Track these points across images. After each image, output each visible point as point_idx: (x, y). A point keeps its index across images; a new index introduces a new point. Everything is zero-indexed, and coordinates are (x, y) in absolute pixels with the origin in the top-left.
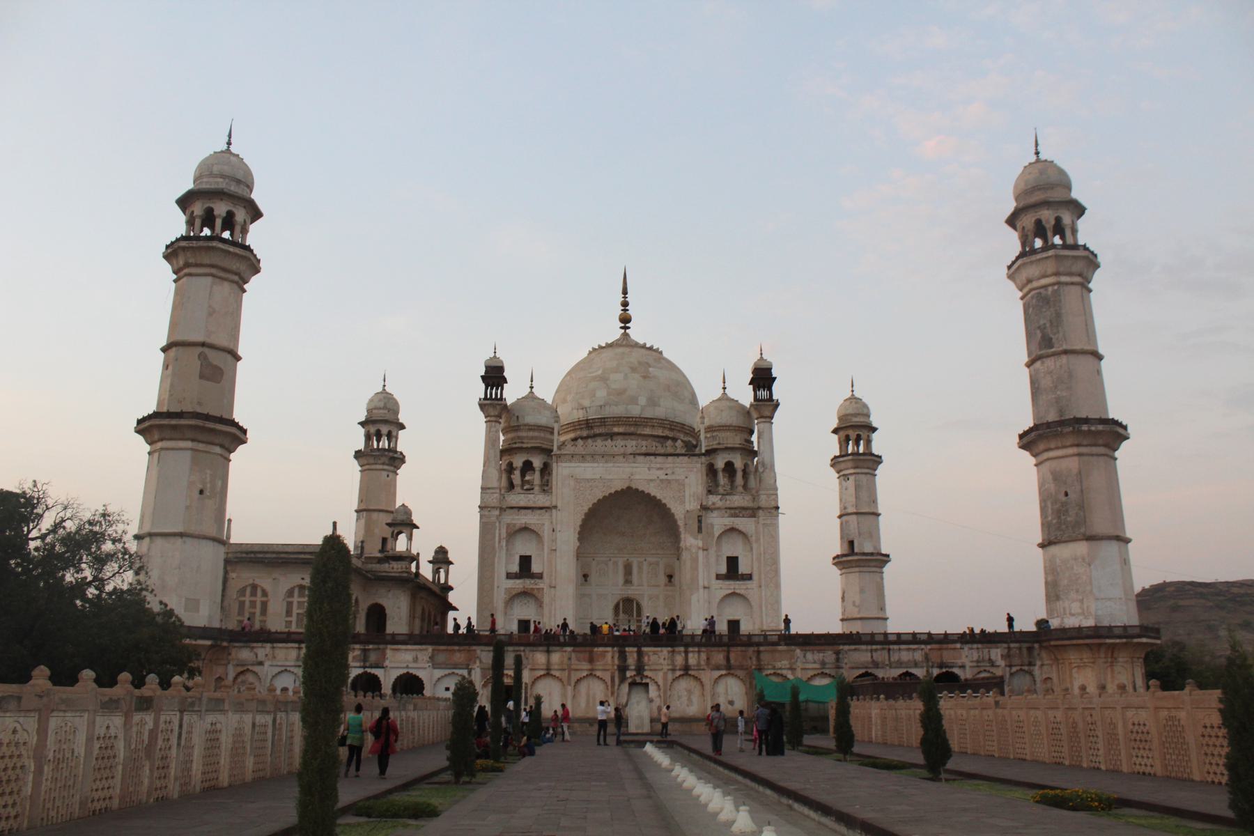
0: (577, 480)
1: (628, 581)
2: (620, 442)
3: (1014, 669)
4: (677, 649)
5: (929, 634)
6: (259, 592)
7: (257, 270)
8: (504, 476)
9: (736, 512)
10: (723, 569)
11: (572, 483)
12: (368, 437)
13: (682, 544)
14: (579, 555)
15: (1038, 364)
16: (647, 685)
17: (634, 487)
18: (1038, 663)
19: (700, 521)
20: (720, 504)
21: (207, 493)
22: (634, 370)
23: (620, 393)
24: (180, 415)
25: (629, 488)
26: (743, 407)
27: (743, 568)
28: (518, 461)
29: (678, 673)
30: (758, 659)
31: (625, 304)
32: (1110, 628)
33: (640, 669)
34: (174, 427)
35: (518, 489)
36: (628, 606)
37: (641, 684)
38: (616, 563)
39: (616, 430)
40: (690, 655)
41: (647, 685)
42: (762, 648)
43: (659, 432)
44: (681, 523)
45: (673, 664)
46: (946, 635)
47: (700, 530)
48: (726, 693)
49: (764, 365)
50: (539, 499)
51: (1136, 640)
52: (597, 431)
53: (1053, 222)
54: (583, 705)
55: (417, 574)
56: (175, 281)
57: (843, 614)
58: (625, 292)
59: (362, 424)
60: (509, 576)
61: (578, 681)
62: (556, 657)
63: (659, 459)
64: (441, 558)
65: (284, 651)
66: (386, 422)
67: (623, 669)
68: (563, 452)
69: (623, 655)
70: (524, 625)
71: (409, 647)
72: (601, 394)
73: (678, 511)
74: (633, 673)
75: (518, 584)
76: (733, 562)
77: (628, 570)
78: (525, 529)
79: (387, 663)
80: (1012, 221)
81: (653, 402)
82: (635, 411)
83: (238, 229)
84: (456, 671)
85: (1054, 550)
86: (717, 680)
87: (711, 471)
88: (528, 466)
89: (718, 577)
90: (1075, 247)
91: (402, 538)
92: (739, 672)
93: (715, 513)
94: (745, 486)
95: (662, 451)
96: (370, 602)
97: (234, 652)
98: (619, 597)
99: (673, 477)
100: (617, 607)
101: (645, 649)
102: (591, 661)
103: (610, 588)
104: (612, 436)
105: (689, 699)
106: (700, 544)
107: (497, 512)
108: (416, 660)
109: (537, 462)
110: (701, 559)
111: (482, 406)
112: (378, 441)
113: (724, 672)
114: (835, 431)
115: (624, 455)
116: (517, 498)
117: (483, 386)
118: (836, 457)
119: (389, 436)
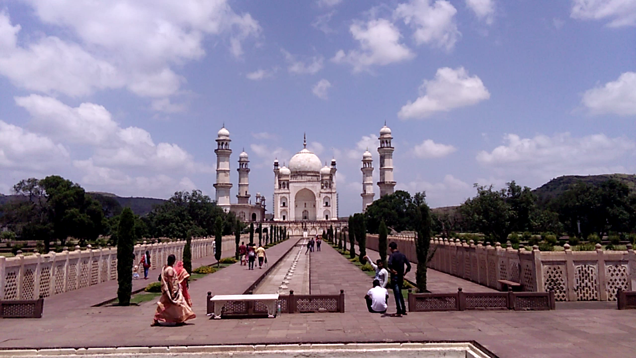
1: (305, 207)
2: (303, 177)
7: (231, 153)
14: (295, 201)
19: (320, 195)
23: (304, 165)
24: (223, 184)
25: (305, 189)
27: (328, 205)
28: (282, 183)
31: (305, 141)
33: (305, 227)
35: (282, 188)
43: (312, 174)
47: (320, 197)
49: (334, 160)
50: (288, 191)
58: (305, 138)
60: (281, 207)
62: (291, 225)
64: (263, 200)
67: (302, 227)
69: (302, 224)
72: (299, 165)
73: (315, 193)
75: (283, 208)
76: (327, 203)
77: (305, 204)
78: (284, 197)
81: (311, 167)
82: (307, 170)
88: (284, 184)
89: (324, 206)
91: (258, 199)
95: (311, 180)
100: (303, 212)
102: (297, 225)
103: (301, 209)
104: (302, 176)
109: (286, 183)
115: (304, 182)
116: (282, 191)
119: (246, 164)
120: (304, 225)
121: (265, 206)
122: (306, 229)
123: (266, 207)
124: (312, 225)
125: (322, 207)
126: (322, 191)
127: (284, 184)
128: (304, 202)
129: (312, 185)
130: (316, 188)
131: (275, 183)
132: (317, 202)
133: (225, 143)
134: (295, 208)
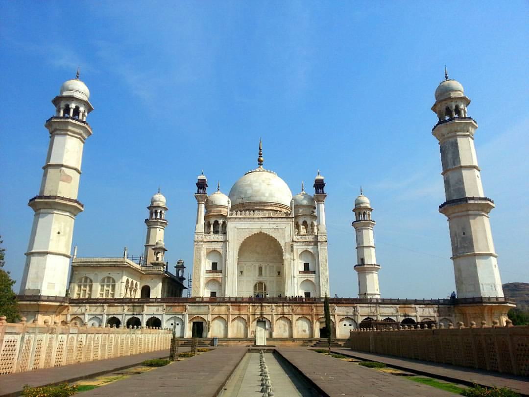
0: (237, 228)
3: (441, 318)
4: (279, 304)
5: (398, 299)
6: (88, 281)
8: (206, 227)
9: (308, 243)
10: (302, 269)
11: (236, 229)
12: (151, 214)
13: (284, 258)
15: (449, 173)
16: (265, 321)
17: (263, 232)
18: (454, 315)
19: (292, 247)
20: (300, 240)
21: (61, 233)
22: (263, 181)
25: (261, 232)
26: (311, 197)
27: (311, 268)
28: (212, 221)
29: (280, 316)
30: (317, 310)
31: (260, 155)
32: (489, 298)
33: (262, 314)
34: (46, 203)
35: (212, 233)
36: (260, 286)
37: (262, 321)
38: (255, 266)
39: (256, 208)
40: (285, 307)
41: (265, 321)
42: (318, 305)
43: (274, 208)
44: (283, 248)
45: (277, 312)
46: (407, 300)
47: (292, 251)
48: (302, 326)
49: (320, 177)
51: (502, 305)
52: (247, 208)
53: (454, 107)
54: (235, 331)
55: (166, 272)
56: (50, 137)
57: (360, 292)
59: (148, 208)
61: (233, 320)
62: (223, 309)
63: (274, 220)
64: (180, 267)
65: (95, 308)
66: (159, 207)
68: (231, 217)
70: (213, 294)
71: (155, 304)
73: (282, 244)
74: (259, 316)
75: (211, 275)
77: (260, 269)
78: (214, 251)
79: (144, 312)
80: (434, 109)
82: (264, 199)
83: (81, 115)
84: (176, 316)
85: (458, 260)
86: (298, 320)
87: (297, 226)
90: (465, 118)
92: (308, 317)
93: (298, 244)
94: (313, 232)
95: (275, 217)
96: (143, 285)
97: (70, 308)
98: (256, 281)
99: (279, 228)
100: (255, 286)
101: (263, 304)
102: (239, 310)
105: (285, 329)
106: (292, 258)
107: (202, 243)
108: (158, 310)
109: (221, 222)
110: (292, 264)
111: (195, 196)
112: (156, 215)
113: (301, 316)
114: (353, 211)
115: (258, 218)
117: (197, 188)
118: (355, 222)
120: (258, 312)
121: (183, 279)
122: (261, 321)
123: (184, 281)
124: (280, 310)
125: (296, 274)
126: (295, 239)
127: (216, 225)
128: (257, 265)
129: (274, 226)
130: (283, 232)
131: (197, 223)
132: (286, 263)
133: (73, 106)
134: (239, 276)
